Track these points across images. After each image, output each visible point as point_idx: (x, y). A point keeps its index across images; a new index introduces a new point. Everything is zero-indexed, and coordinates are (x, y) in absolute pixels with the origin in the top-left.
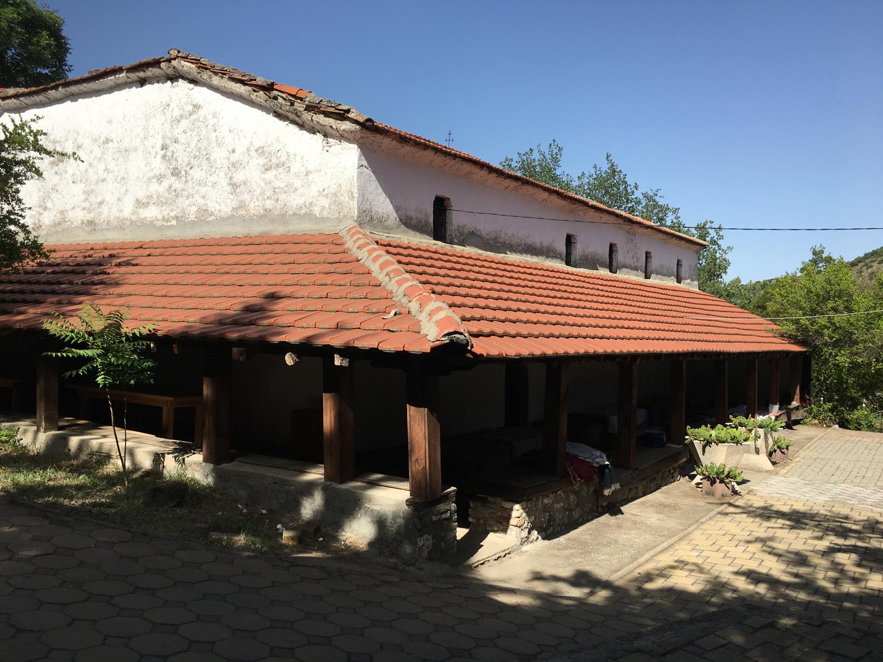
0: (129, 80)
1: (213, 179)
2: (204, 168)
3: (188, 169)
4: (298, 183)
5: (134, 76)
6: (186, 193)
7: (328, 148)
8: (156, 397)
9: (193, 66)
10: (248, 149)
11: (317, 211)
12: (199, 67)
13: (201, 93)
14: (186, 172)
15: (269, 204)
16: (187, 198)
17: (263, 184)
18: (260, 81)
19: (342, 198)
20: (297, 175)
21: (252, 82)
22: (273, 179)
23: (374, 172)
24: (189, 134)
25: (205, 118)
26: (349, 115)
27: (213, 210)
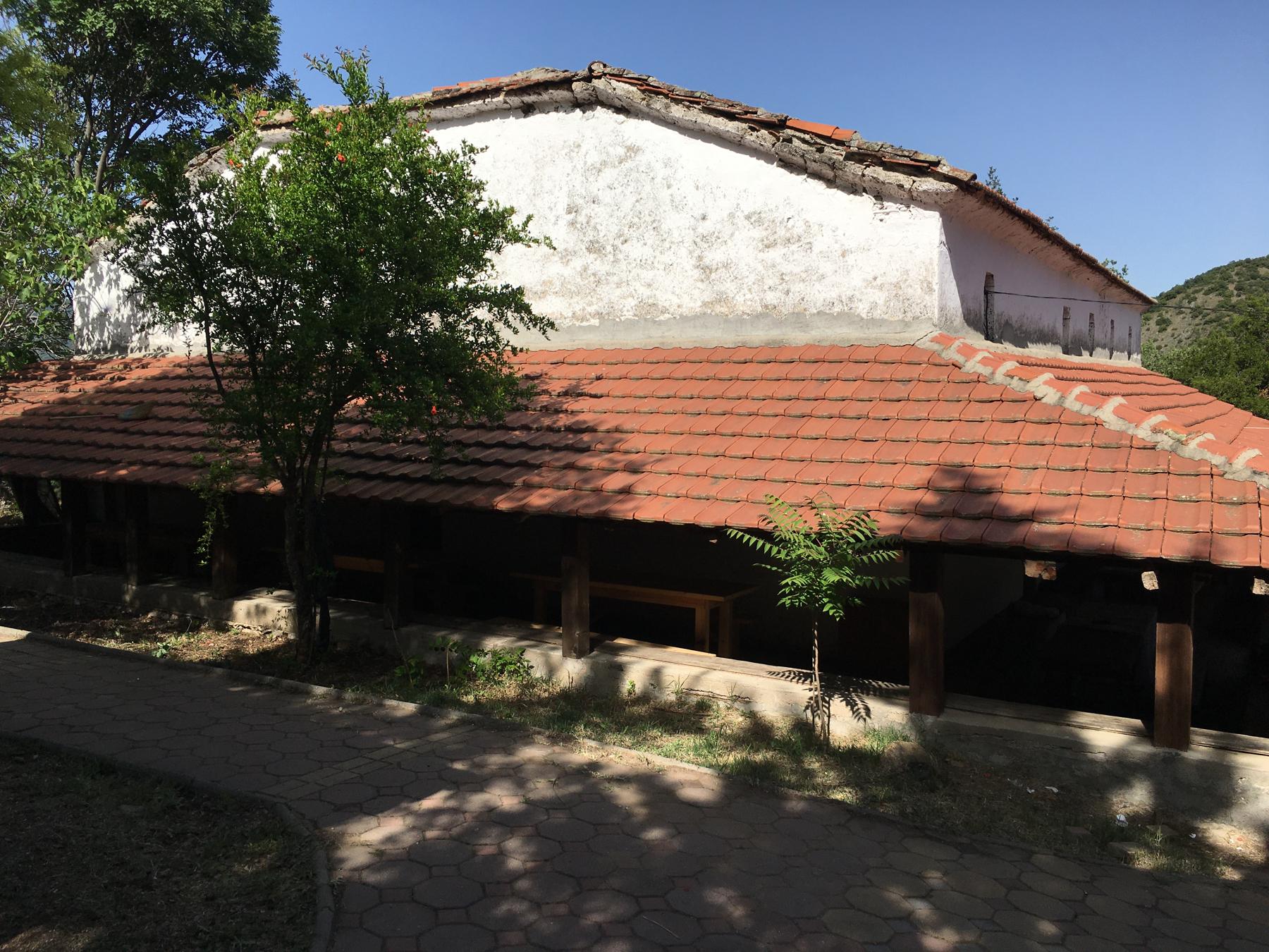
0: (506, 106)
1: (666, 258)
2: (649, 242)
3: (618, 242)
4: (826, 267)
5: (515, 101)
6: (615, 279)
7: (883, 217)
8: (689, 595)
9: (634, 89)
10: (732, 215)
11: (862, 309)
12: (643, 91)
13: (645, 128)
14: (615, 248)
15: (771, 298)
16: (619, 285)
17: (760, 268)
18: (763, 114)
19: (910, 291)
20: (825, 255)
21: (748, 116)
22: (779, 260)
23: (949, 250)
24: (619, 191)
25: (649, 166)
26: (939, 169)
27: (667, 304)
